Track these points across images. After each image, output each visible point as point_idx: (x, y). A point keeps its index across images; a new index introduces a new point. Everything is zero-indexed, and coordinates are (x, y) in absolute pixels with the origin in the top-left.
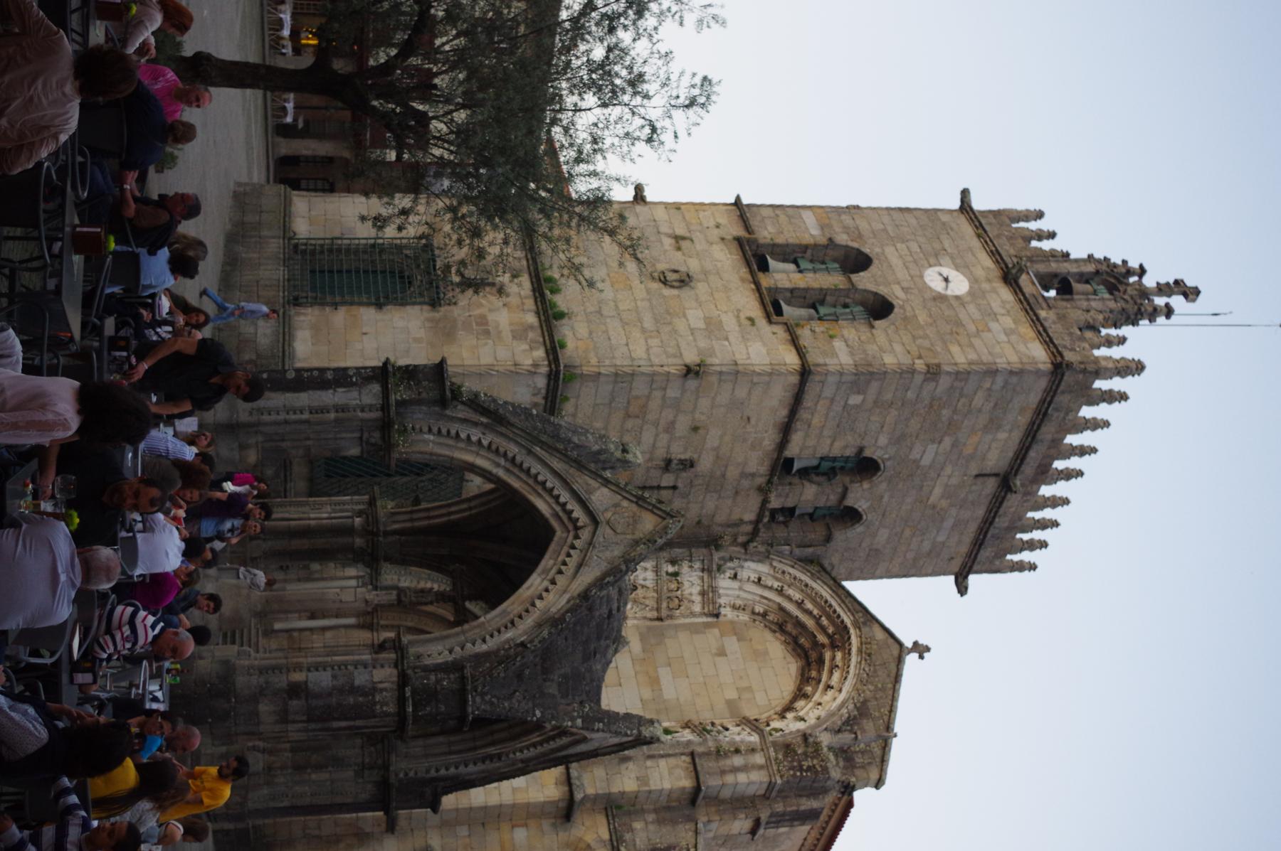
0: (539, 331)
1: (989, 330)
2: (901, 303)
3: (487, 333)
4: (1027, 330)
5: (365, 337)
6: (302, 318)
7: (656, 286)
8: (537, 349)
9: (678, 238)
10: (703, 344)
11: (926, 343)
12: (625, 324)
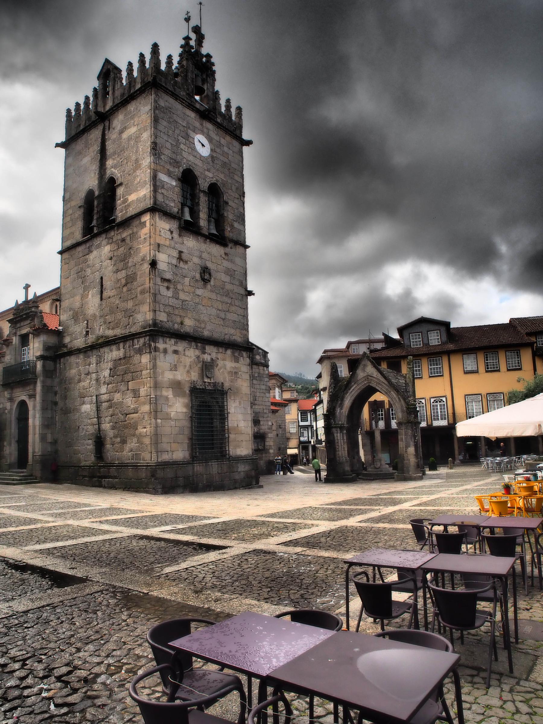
0: (235, 350)
1: (228, 154)
2: (215, 179)
3: (236, 373)
4: (228, 138)
5: (239, 426)
6: (231, 453)
7: (209, 287)
8: (242, 354)
9: (180, 259)
10: (237, 283)
11: (234, 188)
12: (228, 311)
